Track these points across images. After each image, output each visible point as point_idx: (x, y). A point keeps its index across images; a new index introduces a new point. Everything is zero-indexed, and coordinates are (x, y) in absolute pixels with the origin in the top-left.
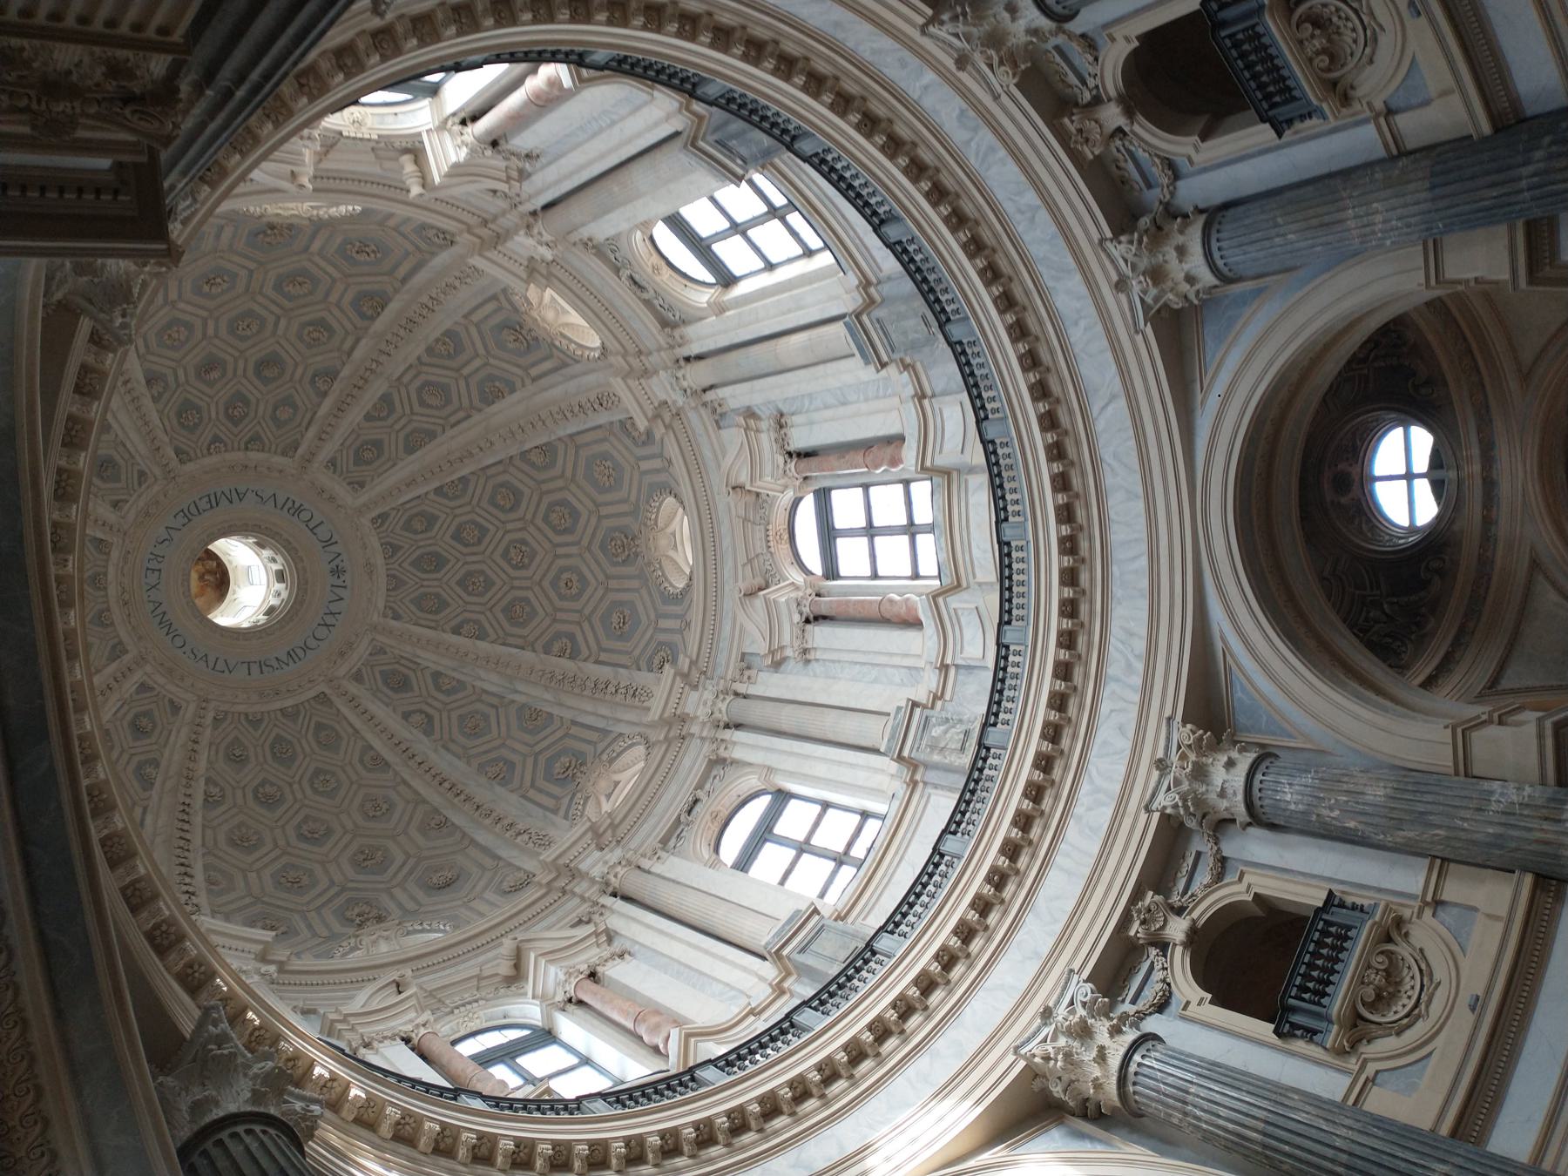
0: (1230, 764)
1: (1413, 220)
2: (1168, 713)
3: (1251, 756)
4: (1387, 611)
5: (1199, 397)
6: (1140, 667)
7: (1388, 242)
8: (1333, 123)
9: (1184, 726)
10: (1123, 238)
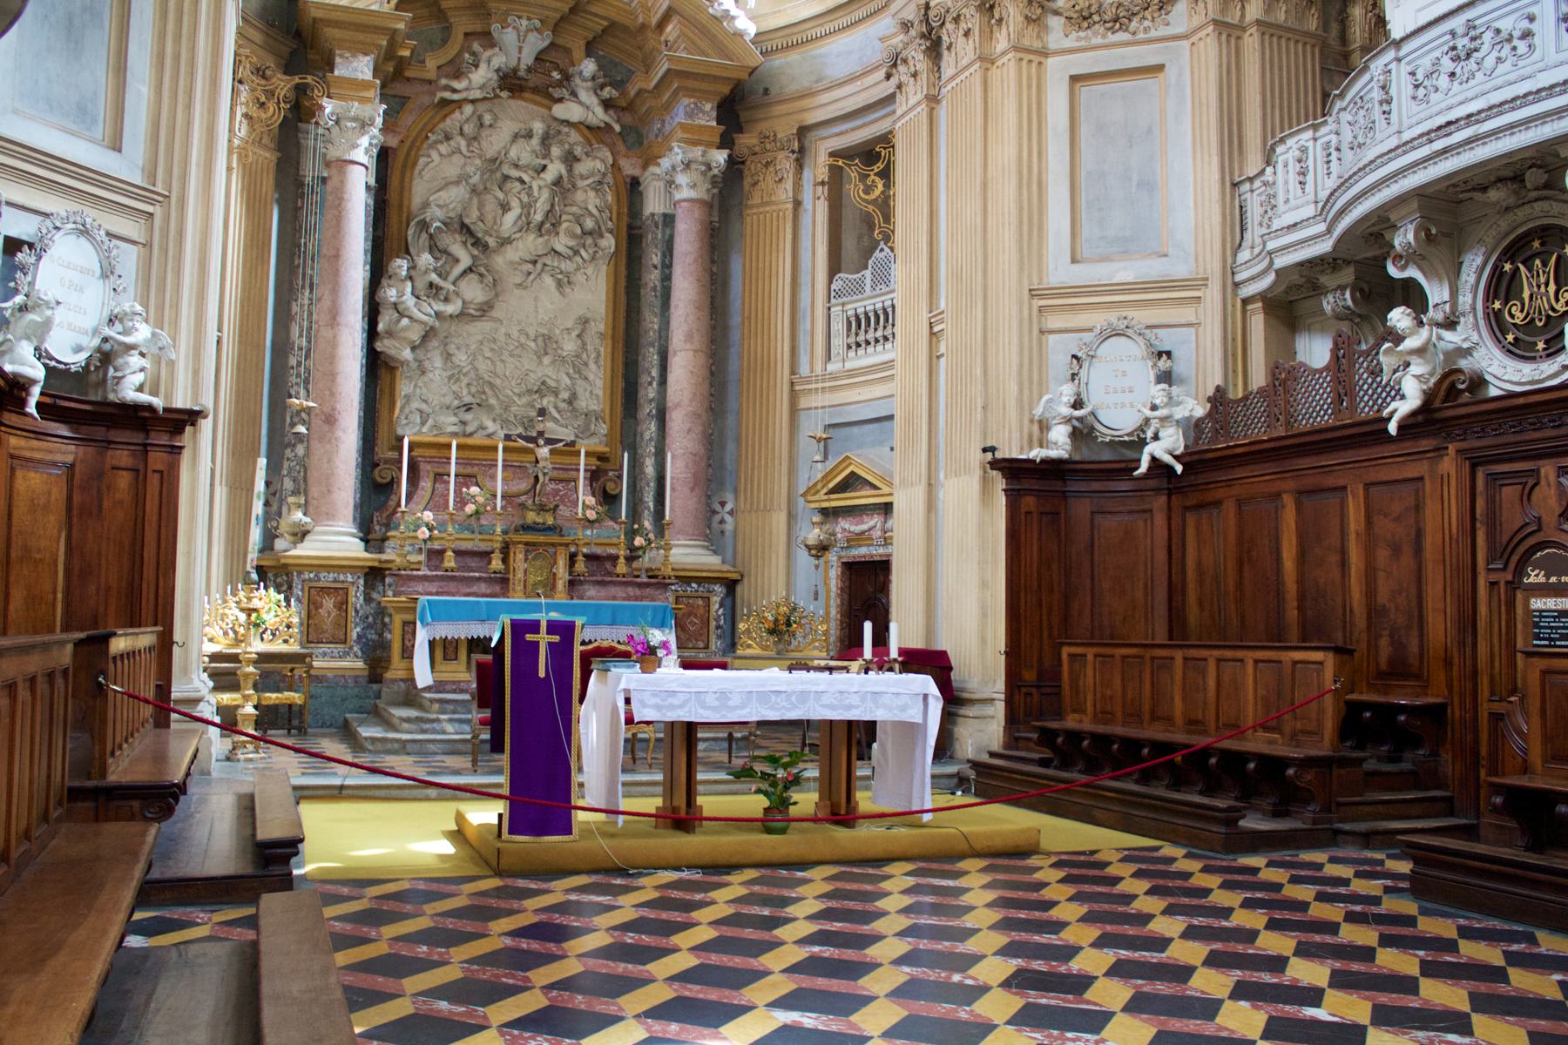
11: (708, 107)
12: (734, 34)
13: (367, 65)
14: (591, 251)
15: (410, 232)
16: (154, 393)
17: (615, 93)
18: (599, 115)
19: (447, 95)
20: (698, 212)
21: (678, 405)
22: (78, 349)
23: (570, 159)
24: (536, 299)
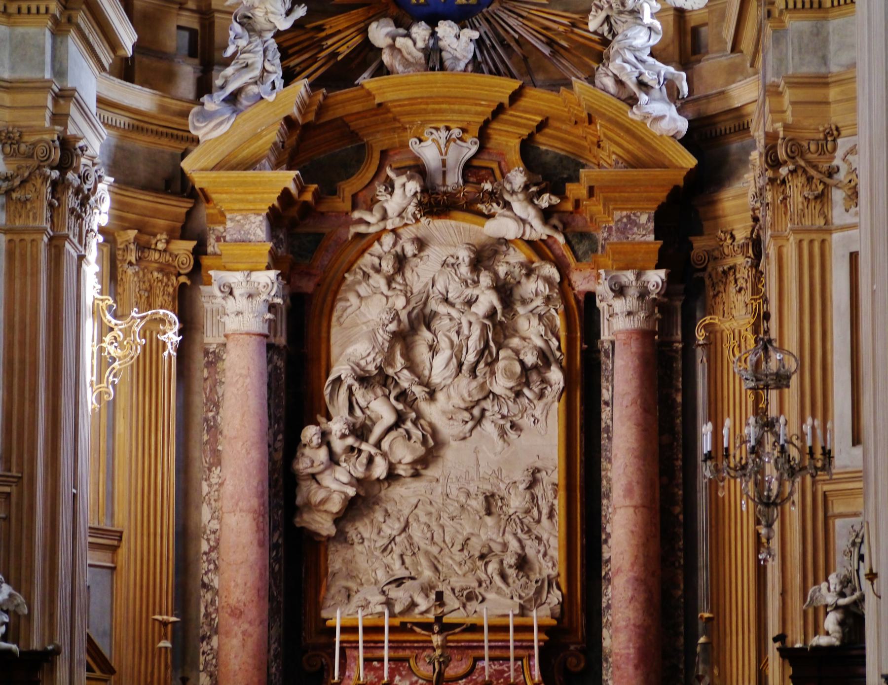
11: (644, 219)
12: (661, 136)
13: (259, 226)
14: (536, 390)
15: (327, 392)
16: (16, 641)
17: (555, 200)
18: (539, 230)
19: (362, 229)
20: (634, 347)
21: (619, 570)
24: (476, 451)
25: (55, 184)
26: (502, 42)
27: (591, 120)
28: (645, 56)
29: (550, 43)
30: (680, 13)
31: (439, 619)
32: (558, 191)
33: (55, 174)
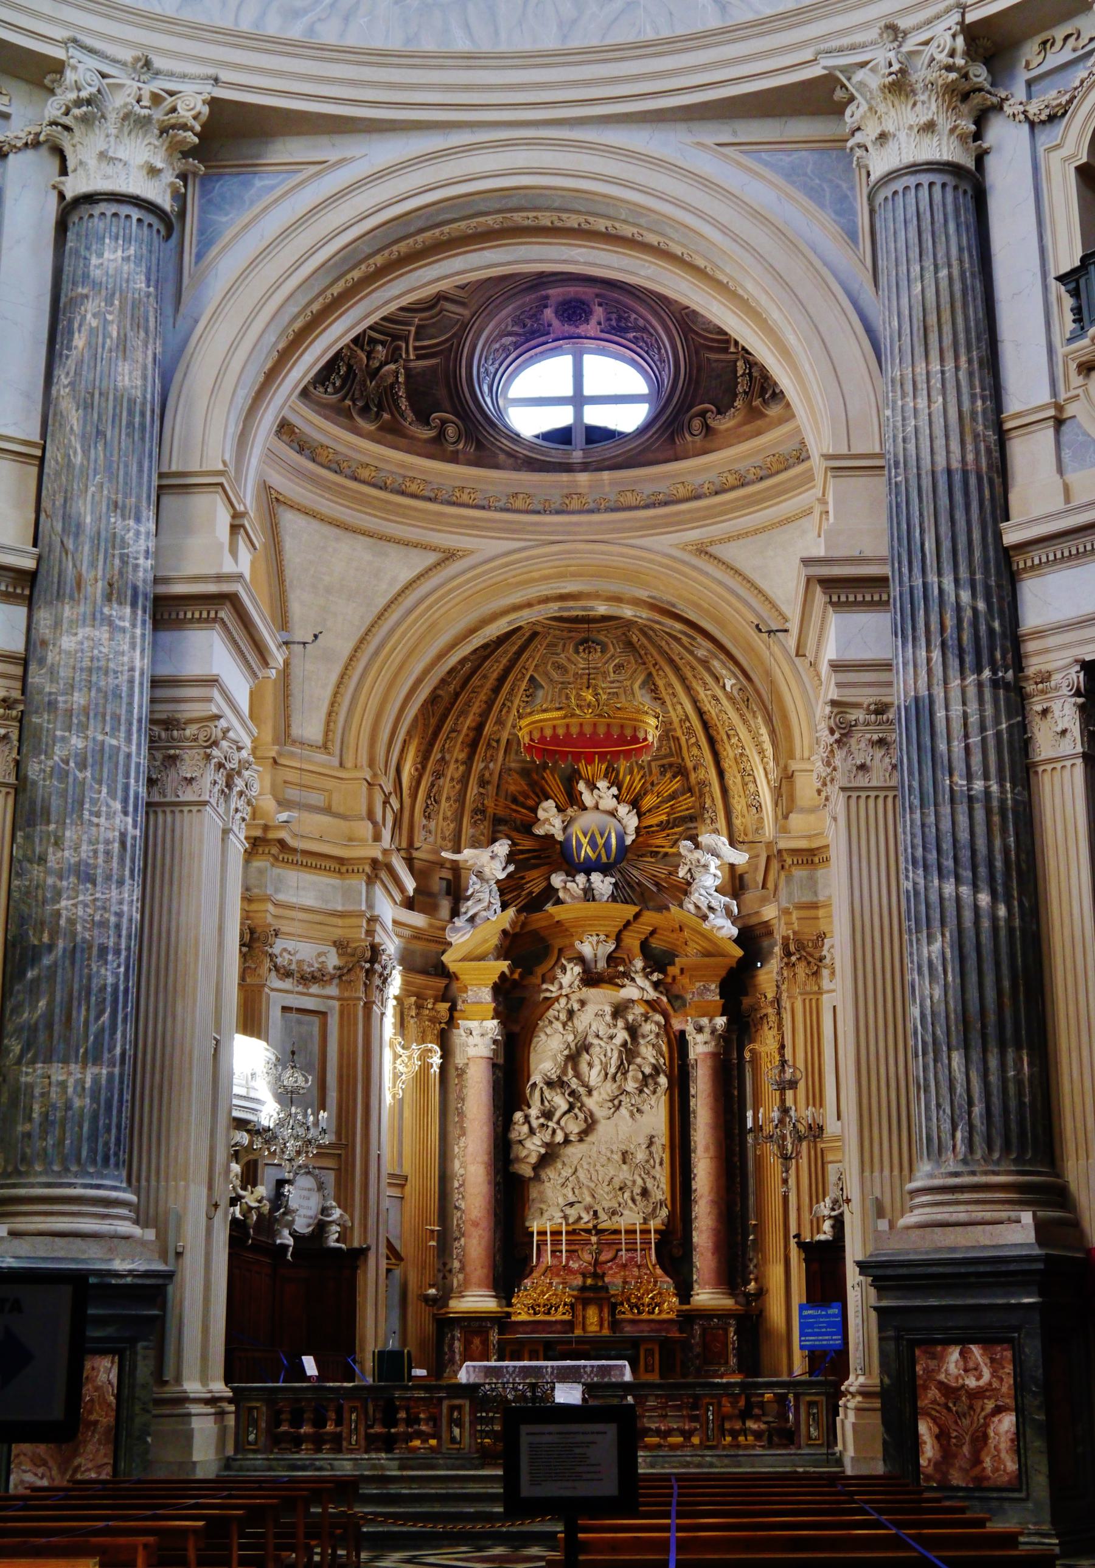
0: (153, 172)
1: (911, 446)
2: (225, 76)
3: (166, 202)
4: (387, 368)
5: (710, 140)
6: (296, 31)
7: (888, 413)
8: (1061, 350)
9: (204, 102)
10: (960, 41)
11: (713, 987)
15: (528, 1091)
17: (661, 976)
18: (652, 994)
19: (548, 995)
20: (709, 1062)
22: (309, 1226)
23: (633, 1031)
25: (367, 971)
26: (629, 884)
27: (681, 929)
28: (712, 892)
29: (657, 884)
30: (732, 866)
31: (595, 1227)
32: (663, 970)
33: (368, 965)
